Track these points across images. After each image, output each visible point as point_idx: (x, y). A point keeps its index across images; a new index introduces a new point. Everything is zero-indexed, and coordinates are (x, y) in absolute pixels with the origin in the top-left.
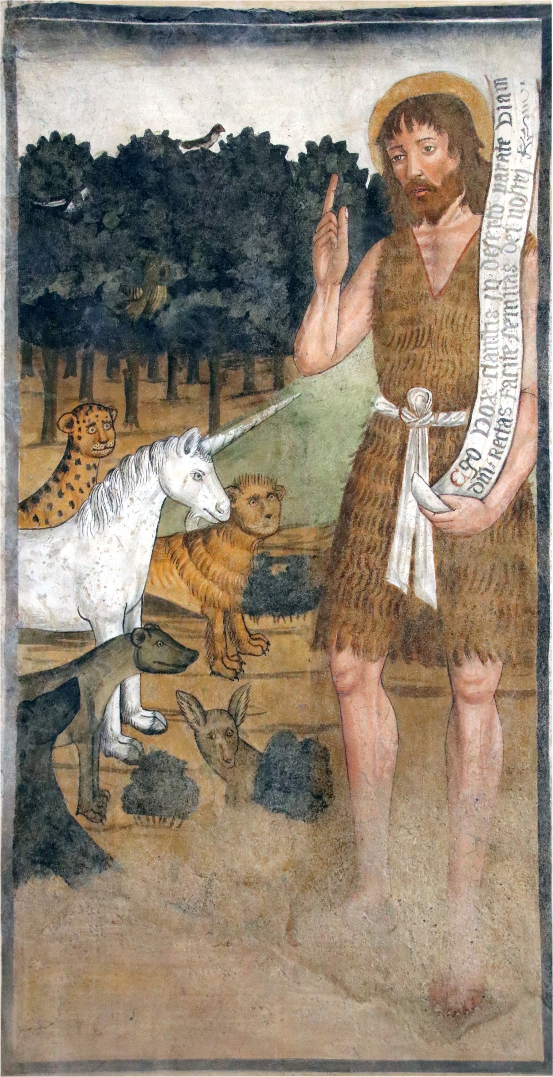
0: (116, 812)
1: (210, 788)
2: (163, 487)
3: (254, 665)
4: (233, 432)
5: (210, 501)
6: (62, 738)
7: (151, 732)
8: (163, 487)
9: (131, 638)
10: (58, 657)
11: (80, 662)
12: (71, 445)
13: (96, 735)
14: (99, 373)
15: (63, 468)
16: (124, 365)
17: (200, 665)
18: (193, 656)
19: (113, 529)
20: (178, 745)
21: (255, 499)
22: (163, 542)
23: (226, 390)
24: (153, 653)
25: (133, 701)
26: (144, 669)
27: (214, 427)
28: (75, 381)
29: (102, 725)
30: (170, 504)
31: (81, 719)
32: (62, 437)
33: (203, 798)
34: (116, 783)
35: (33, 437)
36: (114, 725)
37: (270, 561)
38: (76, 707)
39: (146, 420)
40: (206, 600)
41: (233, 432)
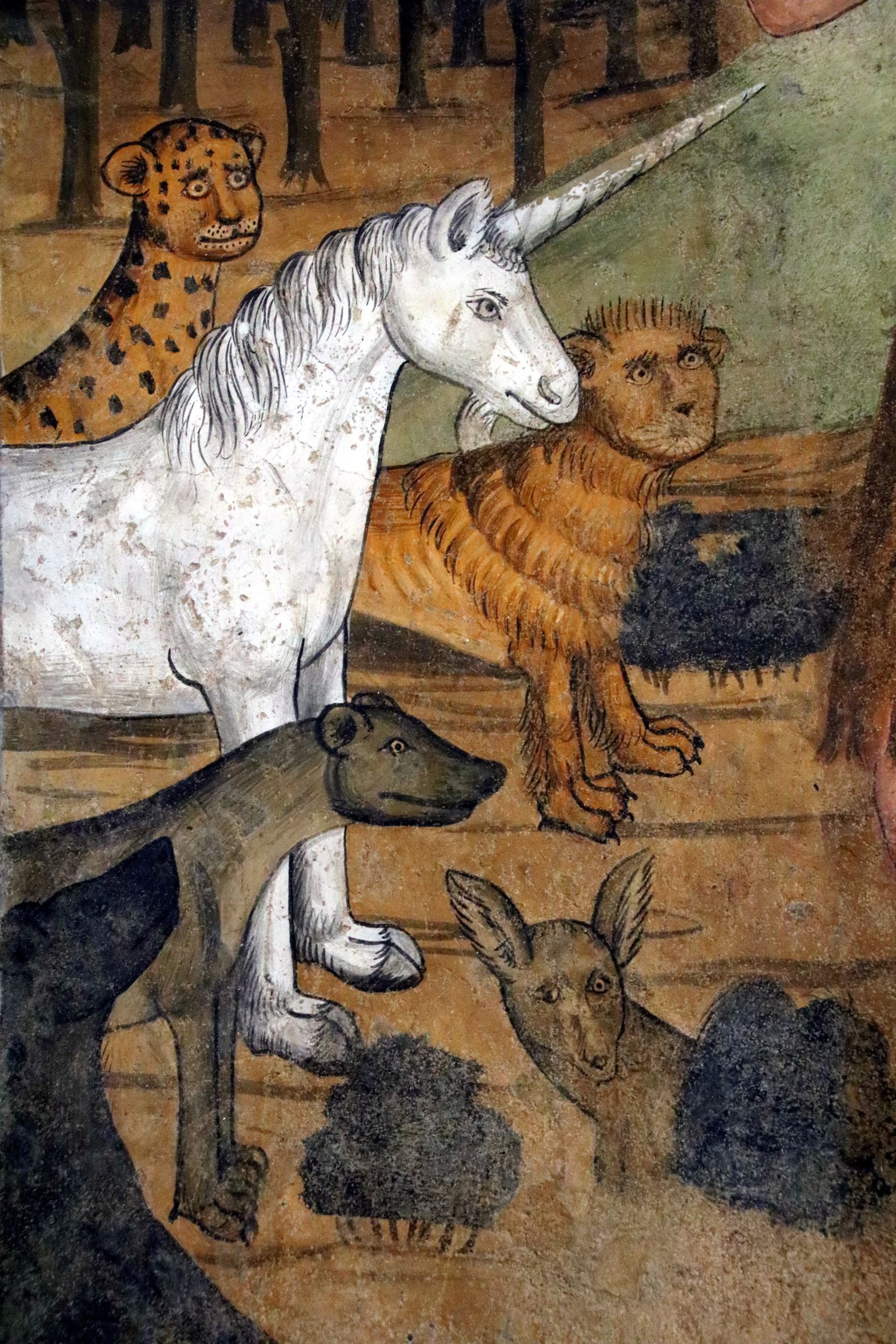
0: (285, 1210)
1: (551, 1139)
2: (395, 336)
3: (659, 801)
4: (579, 192)
5: (522, 370)
6: (129, 1004)
7: (378, 983)
8: (395, 336)
9: (317, 731)
10: (116, 784)
11: (177, 796)
12: (141, 228)
13: (228, 989)
14: (211, 45)
15: (120, 286)
16: (278, 19)
17: (509, 802)
18: (491, 777)
19: (261, 448)
20: (454, 1020)
21: (645, 364)
22: (399, 483)
23: (560, 82)
24: (376, 770)
25: (327, 899)
26: (354, 814)
27: (528, 181)
28: (147, 60)
29: (243, 964)
30: (416, 379)
31: (181, 950)
32: (116, 207)
33: (533, 1167)
34: (284, 1126)
35: (37, 205)
36: (276, 966)
37: (694, 525)
38: (166, 918)
39: (343, 167)
40: (522, 631)
41: (579, 192)
